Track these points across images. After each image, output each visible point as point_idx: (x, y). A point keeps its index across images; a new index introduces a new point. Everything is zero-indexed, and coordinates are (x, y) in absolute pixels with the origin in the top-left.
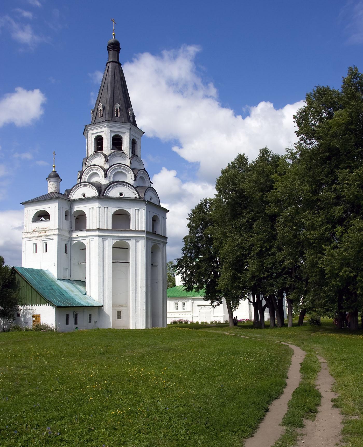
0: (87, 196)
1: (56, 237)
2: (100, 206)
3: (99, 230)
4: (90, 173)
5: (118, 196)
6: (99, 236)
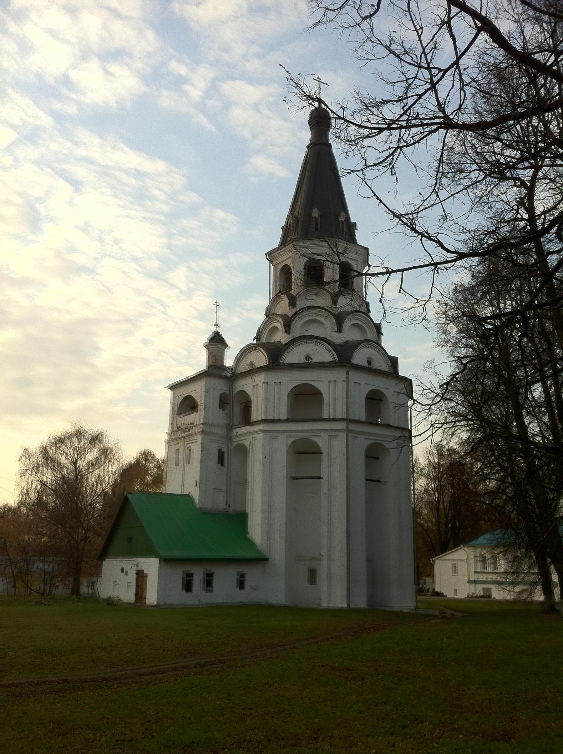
0: (257, 365)
1: (199, 438)
2: (266, 381)
3: (264, 421)
4: (270, 327)
5: (302, 360)
6: (264, 431)
